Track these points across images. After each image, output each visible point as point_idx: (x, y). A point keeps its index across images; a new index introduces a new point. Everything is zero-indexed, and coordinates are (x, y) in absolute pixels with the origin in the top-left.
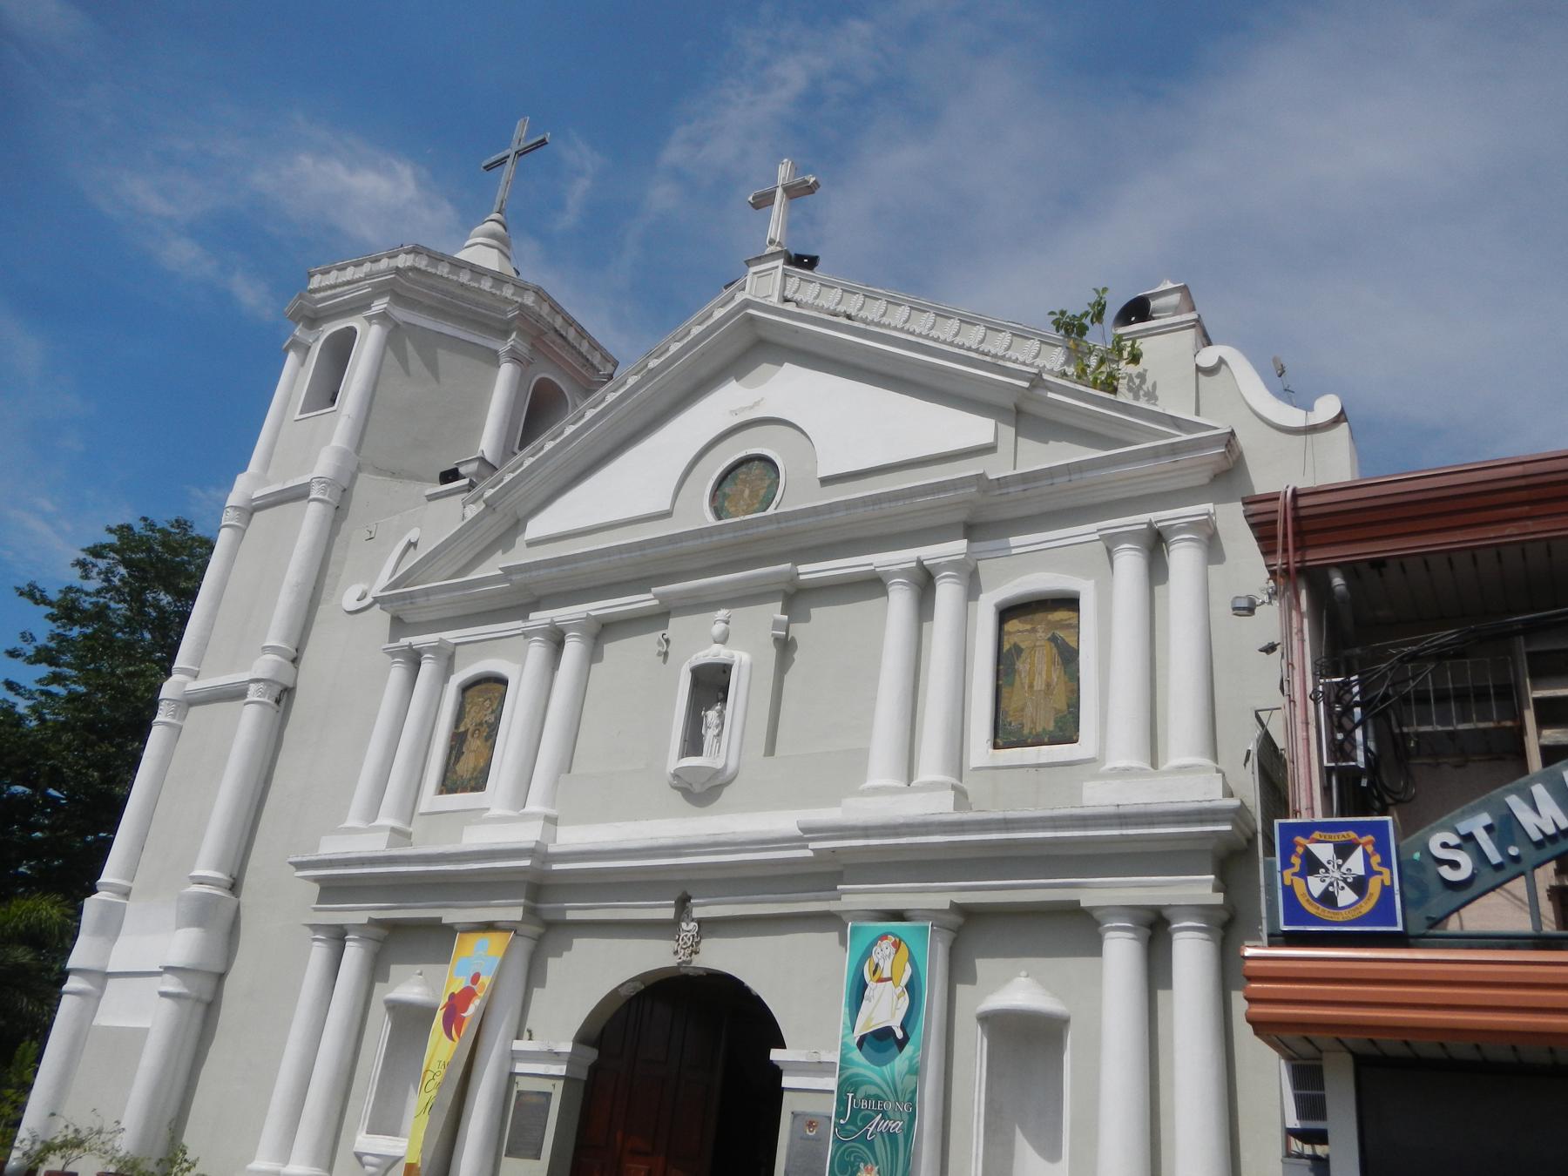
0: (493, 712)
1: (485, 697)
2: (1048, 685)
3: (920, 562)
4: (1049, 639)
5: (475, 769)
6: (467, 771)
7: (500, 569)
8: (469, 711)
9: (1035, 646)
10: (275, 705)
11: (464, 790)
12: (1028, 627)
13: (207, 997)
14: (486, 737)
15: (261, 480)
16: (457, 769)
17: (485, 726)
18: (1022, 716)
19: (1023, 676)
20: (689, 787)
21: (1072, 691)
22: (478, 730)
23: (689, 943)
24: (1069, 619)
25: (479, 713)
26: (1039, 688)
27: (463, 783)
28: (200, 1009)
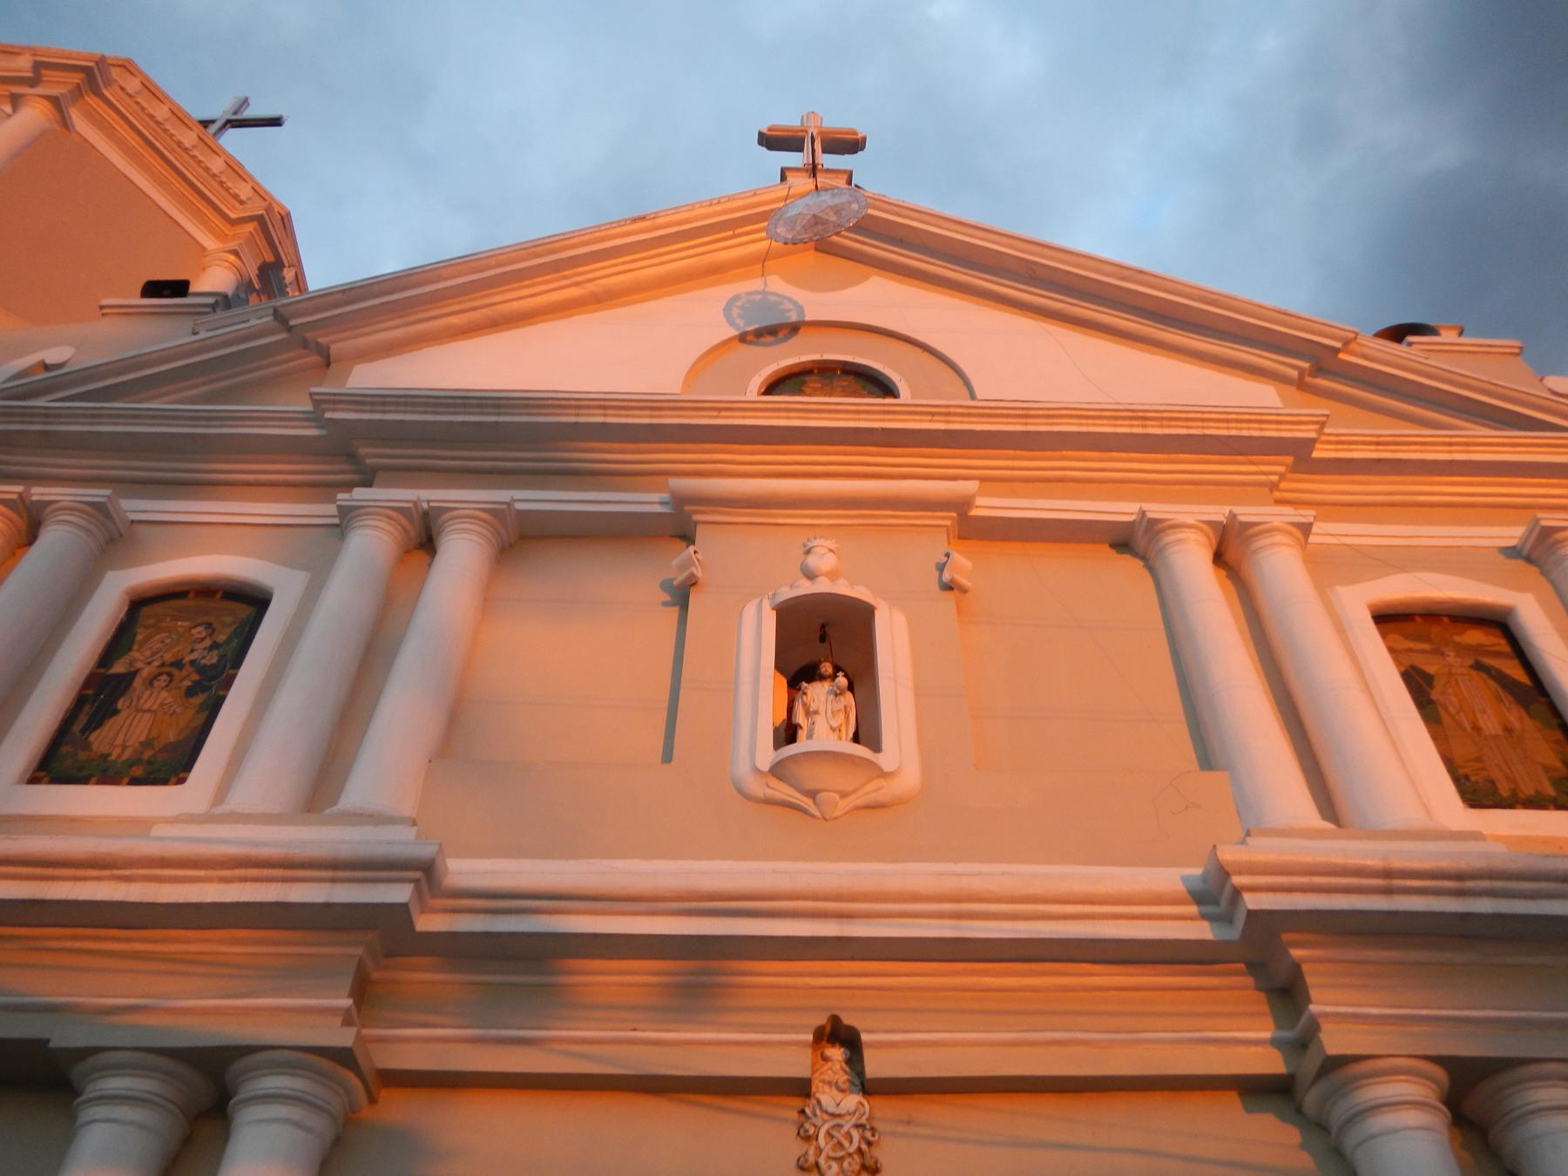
0: (215, 646)
1: (200, 620)
2: (1508, 730)
3: (1233, 516)
4: (1471, 667)
5: (147, 744)
6: (124, 747)
7: (311, 394)
8: (147, 639)
9: (1450, 674)
12: (1426, 646)
14: (188, 688)
17: (188, 669)
18: (1484, 769)
19: (1452, 710)
20: (806, 803)
21: (1556, 742)
22: (169, 674)
23: (852, 1149)
24: (1494, 645)
26: (1493, 732)
27: (105, 771)
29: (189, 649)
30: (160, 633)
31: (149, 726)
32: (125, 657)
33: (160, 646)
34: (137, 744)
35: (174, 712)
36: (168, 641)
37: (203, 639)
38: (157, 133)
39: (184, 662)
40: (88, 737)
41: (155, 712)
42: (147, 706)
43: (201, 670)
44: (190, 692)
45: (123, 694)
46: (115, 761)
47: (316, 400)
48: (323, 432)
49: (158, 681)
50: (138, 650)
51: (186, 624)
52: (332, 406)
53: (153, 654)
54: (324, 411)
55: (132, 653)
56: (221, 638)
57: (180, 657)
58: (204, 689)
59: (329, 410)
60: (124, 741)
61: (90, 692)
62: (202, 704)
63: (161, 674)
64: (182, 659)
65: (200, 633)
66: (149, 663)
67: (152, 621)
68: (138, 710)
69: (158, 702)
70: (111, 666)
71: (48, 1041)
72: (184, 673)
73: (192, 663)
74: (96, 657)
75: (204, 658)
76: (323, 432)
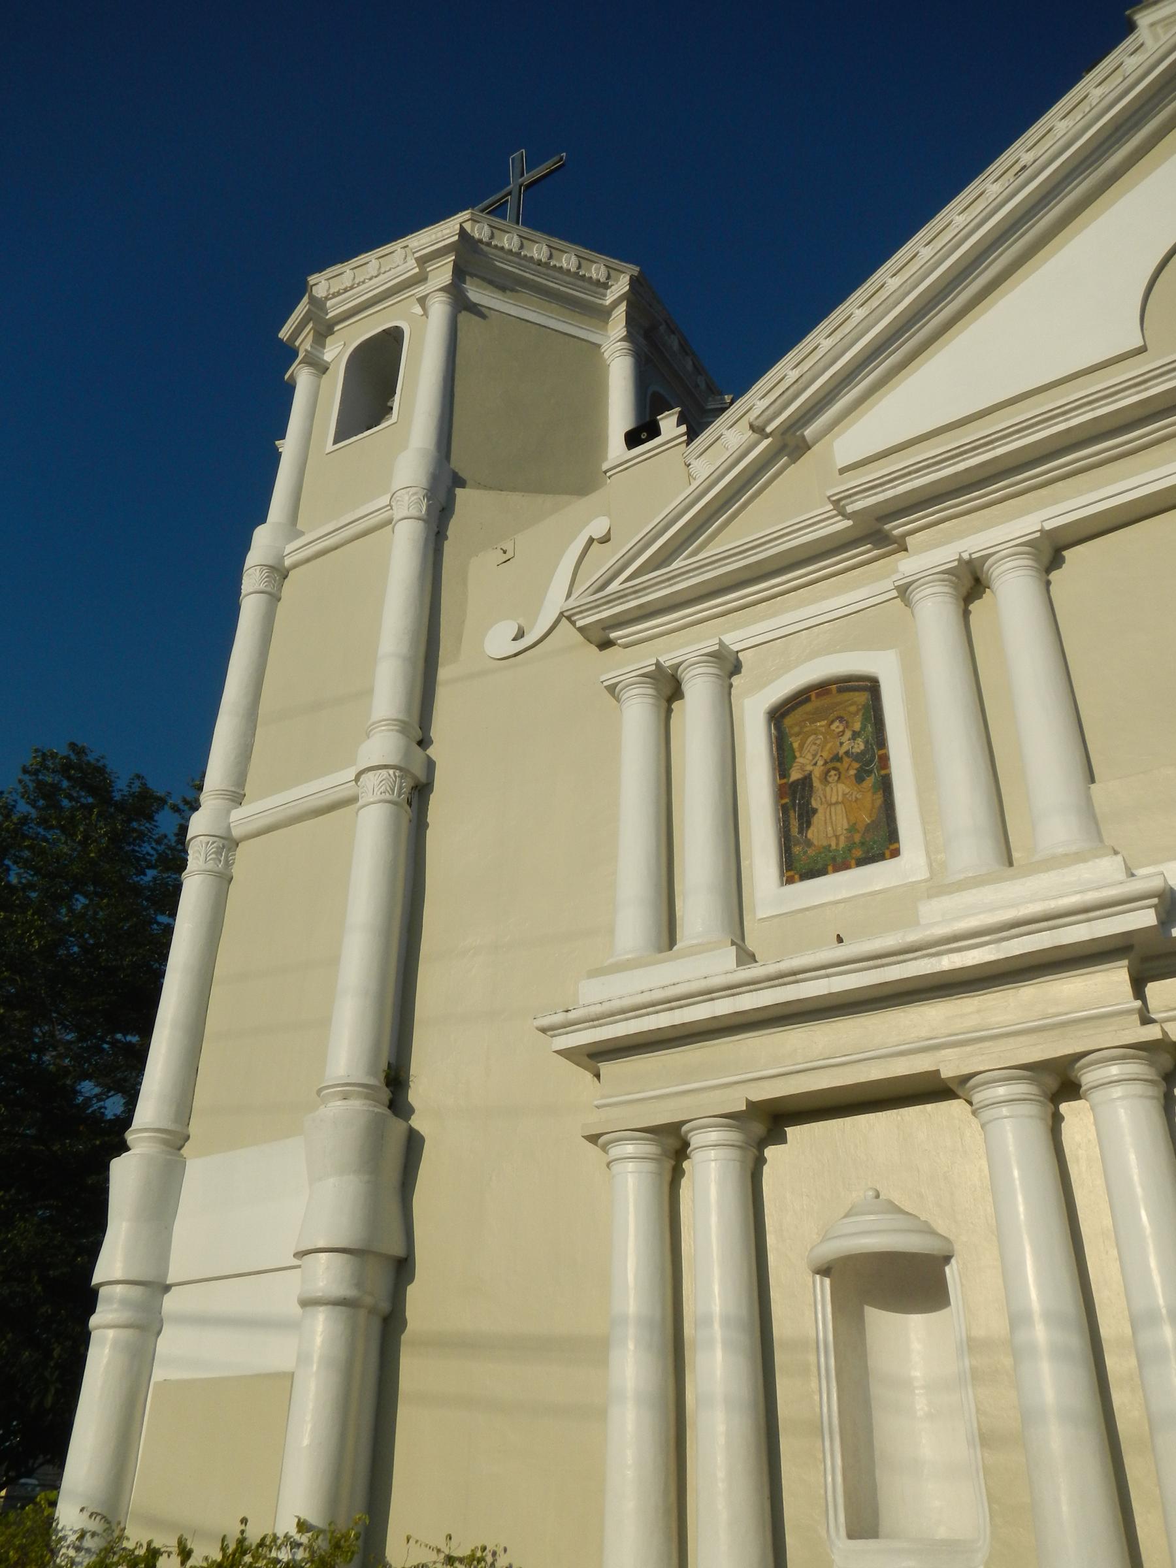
0: (855, 735)
1: (832, 717)
5: (852, 829)
6: (837, 837)
7: (829, 498)
8: (801, 746)
10: (407, 807)
11: (841, 865)
13: (385, 1306)
14: (856, 775)
15: (292, 527)
16: (810, 835)
17: (846, 760)
22: (835, 769)
25: (826, 742)
27: (834, 859)
28: (376, 1325)
29: (838, 743)
30: (810, 736)
31: (845, 815)
32: (795, 764)
33: (814, 747)
34: (845, 832)
35: (856, 798)
36: (818, 742)
37: (843, 732)
38: (521, 265)
39: (840, 756)
40: (806, 837)
41: (842, 802)
42: (834, 800)
43: (857, 757)
44: (859, 778)
45: (811, 797)
46: (837, 850)
47: (834, 501)
48: (850, 523)
49: (830, 776)
50: (801, 756)
51: (824, 723)
52: (849, 500)
53: (814, 756)
54: (844, 506)
55: (797, 760)
56: (857, 726)
57: (835, 752)
58: (870, 772)
59: (848, 504)
60: (834, 831)
61: (786, 800)
62: (873, 786)
63: (828, 771)
64: (838, 754)
65: (838, 727)
66: (815, 764)
67: (796, 729)
68: (830, 805)
69: (840, 794)
70: (789, 776)
71: (938, 1071)
72: (846, 765)
73: (847, 753)
74: (774, 769)
75: (852, 748)
76: (850, 523)
